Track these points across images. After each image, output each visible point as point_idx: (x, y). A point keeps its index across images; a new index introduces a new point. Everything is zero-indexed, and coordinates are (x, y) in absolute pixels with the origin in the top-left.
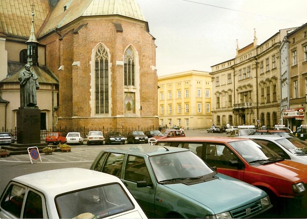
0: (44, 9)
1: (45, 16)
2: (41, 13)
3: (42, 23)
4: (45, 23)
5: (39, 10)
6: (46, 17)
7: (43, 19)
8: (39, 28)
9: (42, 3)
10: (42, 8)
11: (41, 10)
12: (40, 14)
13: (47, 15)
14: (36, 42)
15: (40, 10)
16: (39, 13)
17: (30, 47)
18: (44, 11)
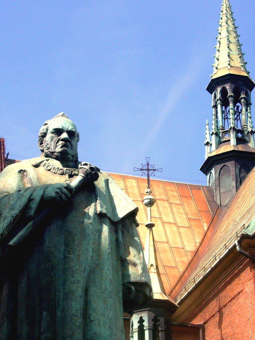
0: (190, 216)
1: (194, 239)
2: (182, 230)
3: (187, 259)
4: (197, 255)
5: (175, 219)
6: (198, 240)
7: (191, 247)
8: (178, 275)
9: (185, 200)
10: (187, 214)
11: (182, 220)
12: (179, 233)
13: (202, 232)
14: (166, 298)
15: (178, 220)
16: (175, 228)
17: (141, 321)
18: (192, 223)
